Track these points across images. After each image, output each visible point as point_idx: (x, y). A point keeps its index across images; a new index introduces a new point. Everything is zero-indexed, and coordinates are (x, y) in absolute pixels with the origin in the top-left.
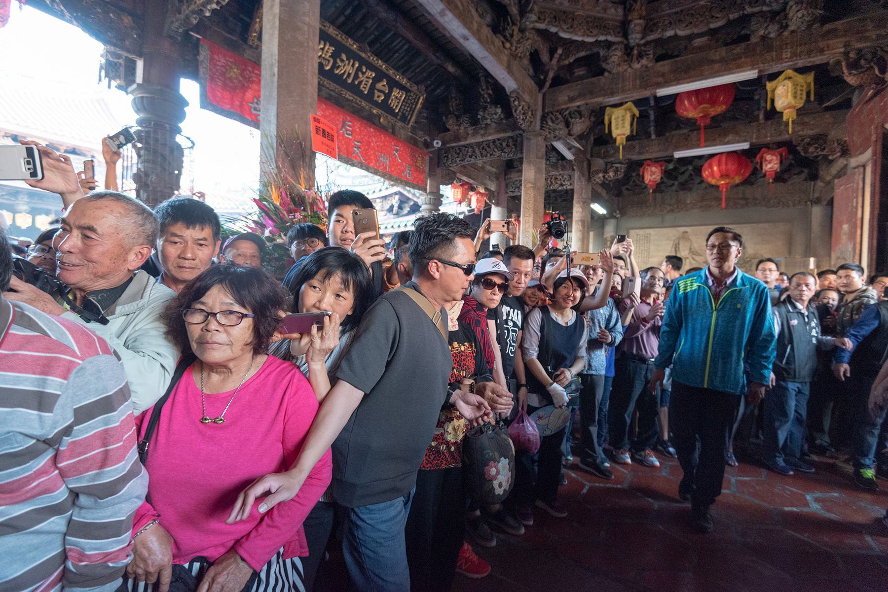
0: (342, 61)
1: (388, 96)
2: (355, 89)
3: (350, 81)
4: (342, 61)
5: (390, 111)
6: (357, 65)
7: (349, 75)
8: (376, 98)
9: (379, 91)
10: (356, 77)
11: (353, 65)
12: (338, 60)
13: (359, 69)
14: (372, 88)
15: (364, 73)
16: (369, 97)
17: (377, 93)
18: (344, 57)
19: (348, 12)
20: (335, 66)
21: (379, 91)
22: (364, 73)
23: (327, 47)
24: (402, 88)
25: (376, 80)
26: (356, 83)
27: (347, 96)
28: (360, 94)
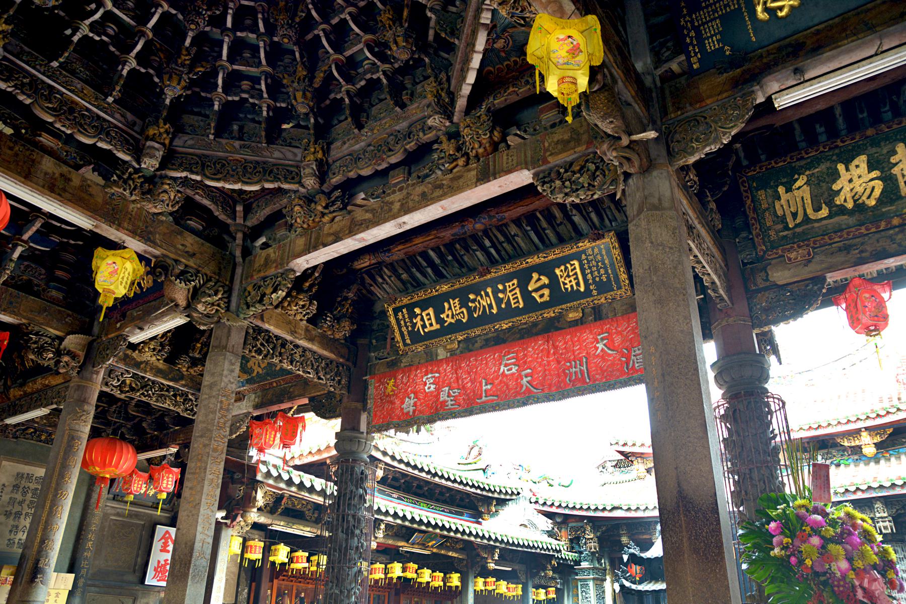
0: (473, 301)
1: (554, 284)
2: (508, 312)
3: (495, 311)
4: (473, 301)
5: (574, 295)
6: (489, 290)
7: (490, 306)
8: (539, 300)
9: (536, 290)
10: (499, 301)
11: (487, 295)
12: (470, 304)
13: (496, 292)
14: (526, 295)
15: (504, 291)
16: (531, 305)
17: (536, 295)
18: (472, 297)
19: (487, 243)
20: (470, 311)
21: (536, 290)
22: (504, 291)
23: (452, 302)
24: (564, 261)
25: (523, 286)
26: (503, 306)
27: (505, 327)
28: (518, 312)
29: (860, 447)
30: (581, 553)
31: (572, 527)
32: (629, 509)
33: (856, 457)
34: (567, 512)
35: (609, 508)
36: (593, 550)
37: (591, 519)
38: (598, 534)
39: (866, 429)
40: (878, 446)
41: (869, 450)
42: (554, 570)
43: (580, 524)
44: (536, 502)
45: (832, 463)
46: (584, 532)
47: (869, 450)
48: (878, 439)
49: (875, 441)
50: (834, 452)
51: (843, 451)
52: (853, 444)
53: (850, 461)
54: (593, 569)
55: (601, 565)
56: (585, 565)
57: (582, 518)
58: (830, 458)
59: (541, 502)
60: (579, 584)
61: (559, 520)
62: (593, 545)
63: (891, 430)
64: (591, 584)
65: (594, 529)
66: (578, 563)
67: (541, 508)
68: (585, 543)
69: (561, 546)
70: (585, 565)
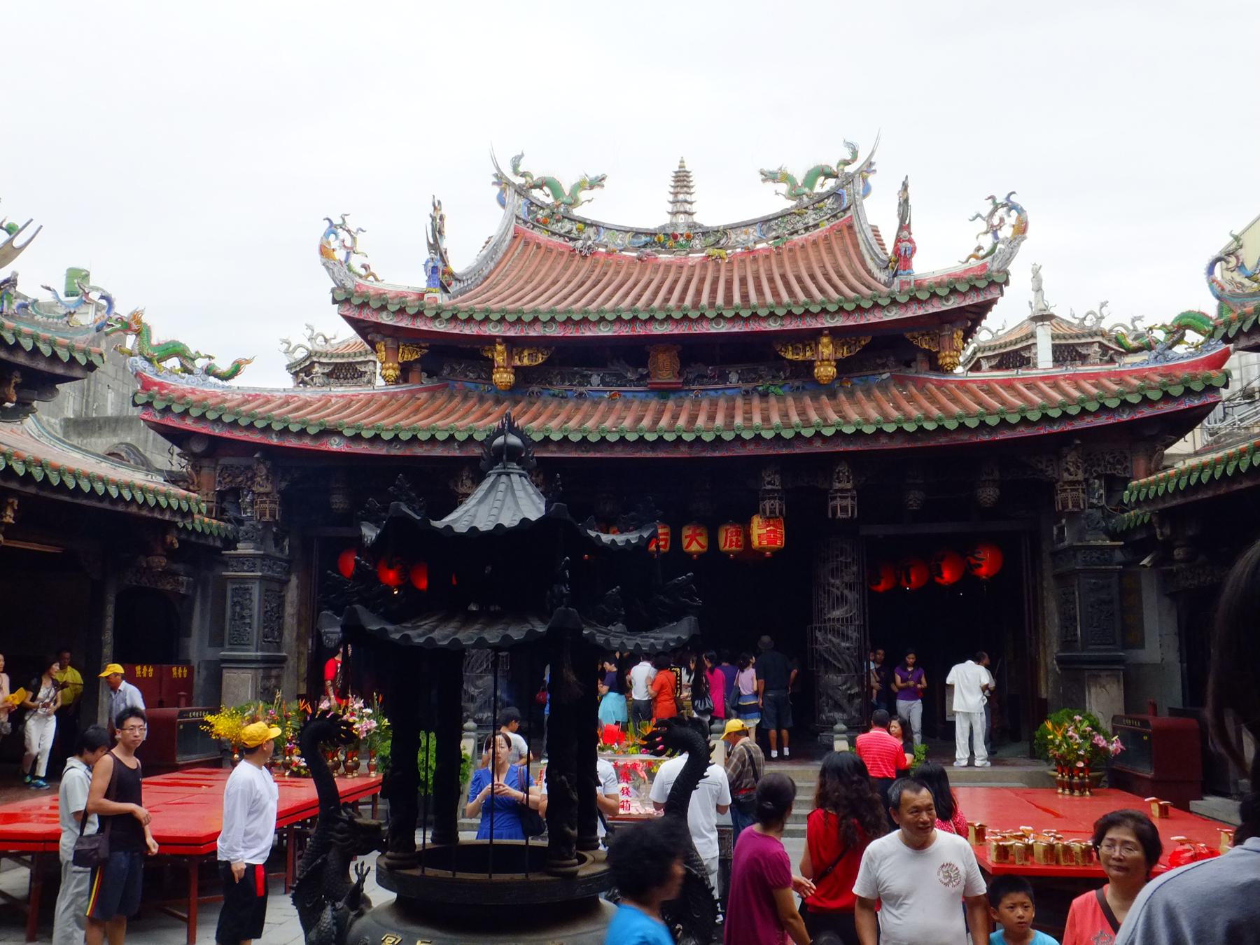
29: (810, 365)
30: (240, 522)
31: (225, 468)
32: (357, 438)
33: (797, 384)
34: (217, 431)
35: (312, 431)
36: (267, 518)
37: (269, 452)
38: (283, 485)
39: (835, 333)
40: (841, 365)
41: (826, 371)
42: (172, 555)
43: (243, 461)
44: (148, 405)
45: (755, 389)
46: (252, 479)
47: (826, 371)
48: (844, 353)
49: (839, 356)
50: (763, 370)
51: (778, 370)
52: (800, 357)
53: (786, 388)
54: (263, 557)
55: (282, 550)
56: (244, 549)
57: (248, 448)
58: (753, 380)
59: (159, 405)
60: (230, 587)
61: (197, 448)
62: (269, 509)
63: (868, 340)
64: (256, 590)
65: (273, 473)
66: (231, 543)
67: (157, 418)
68: (252, 503)
69: (196, 505)
70: (244, 549)
